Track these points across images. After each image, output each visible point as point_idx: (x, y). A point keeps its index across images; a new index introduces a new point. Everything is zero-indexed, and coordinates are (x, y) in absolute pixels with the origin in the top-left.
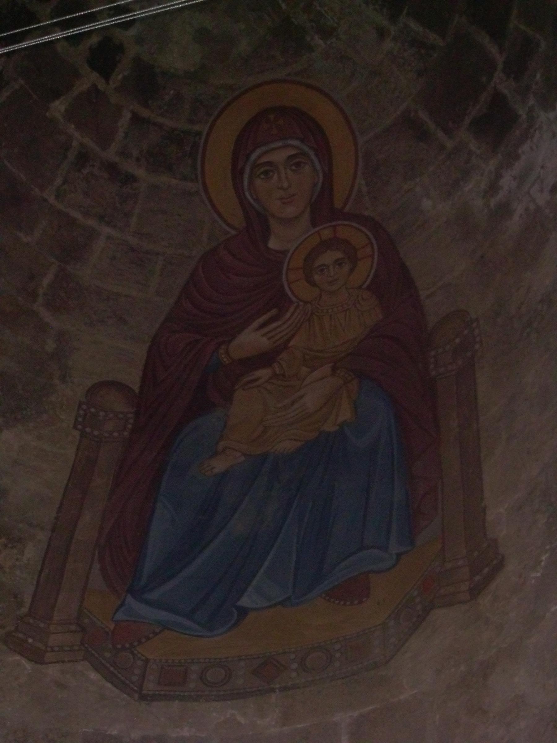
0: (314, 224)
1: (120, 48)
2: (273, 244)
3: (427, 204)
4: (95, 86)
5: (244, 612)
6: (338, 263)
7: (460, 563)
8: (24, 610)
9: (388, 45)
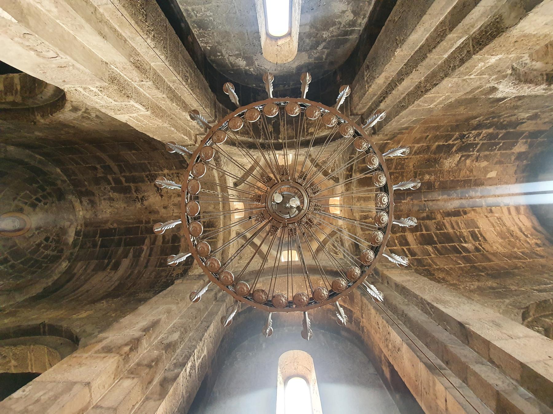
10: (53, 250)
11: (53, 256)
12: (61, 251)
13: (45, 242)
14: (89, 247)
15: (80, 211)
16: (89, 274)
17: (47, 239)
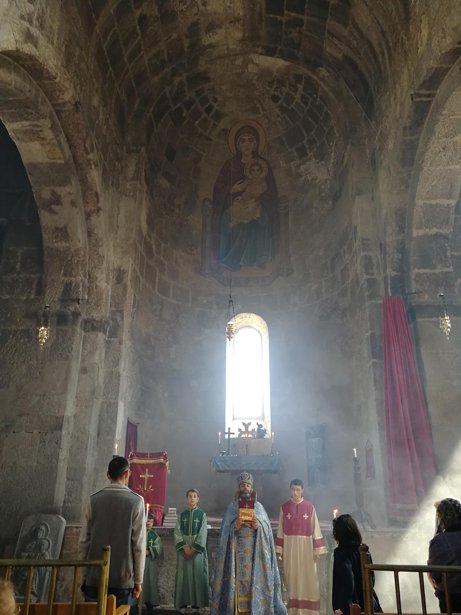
0: (253, 158)
1: (213, 107)
2: (242, 161)
3: (281, 163)
4: (205, 117)
5: (241, 266)
6: (258, 170)
7: (284, 267)
8: (200, 265)
9: (279, 119)
10: (296, 91)
11: (305, 89)
12: (298, 78)
13: (280, 101)
14: (300, 33)
15: (228, 49)
16: (351, 34)
17: (275, 99)
